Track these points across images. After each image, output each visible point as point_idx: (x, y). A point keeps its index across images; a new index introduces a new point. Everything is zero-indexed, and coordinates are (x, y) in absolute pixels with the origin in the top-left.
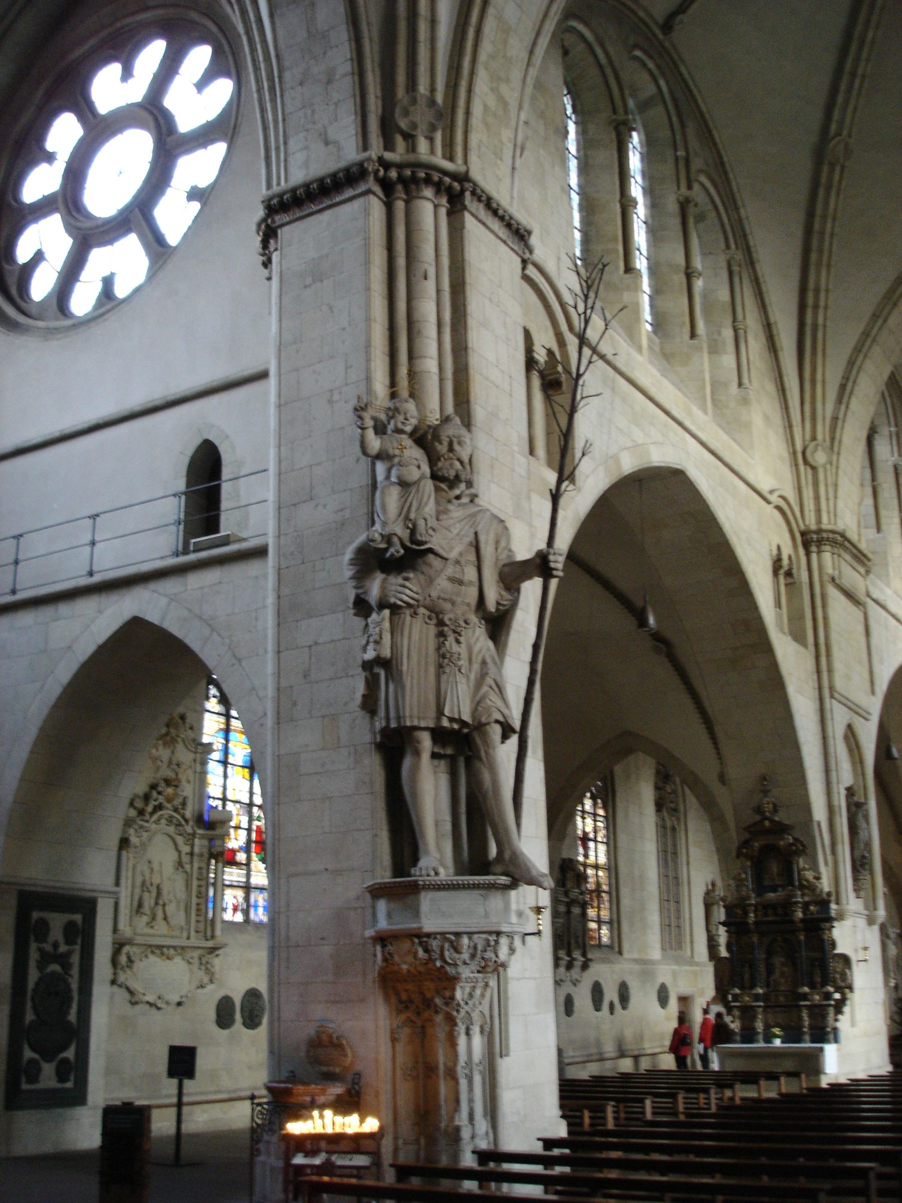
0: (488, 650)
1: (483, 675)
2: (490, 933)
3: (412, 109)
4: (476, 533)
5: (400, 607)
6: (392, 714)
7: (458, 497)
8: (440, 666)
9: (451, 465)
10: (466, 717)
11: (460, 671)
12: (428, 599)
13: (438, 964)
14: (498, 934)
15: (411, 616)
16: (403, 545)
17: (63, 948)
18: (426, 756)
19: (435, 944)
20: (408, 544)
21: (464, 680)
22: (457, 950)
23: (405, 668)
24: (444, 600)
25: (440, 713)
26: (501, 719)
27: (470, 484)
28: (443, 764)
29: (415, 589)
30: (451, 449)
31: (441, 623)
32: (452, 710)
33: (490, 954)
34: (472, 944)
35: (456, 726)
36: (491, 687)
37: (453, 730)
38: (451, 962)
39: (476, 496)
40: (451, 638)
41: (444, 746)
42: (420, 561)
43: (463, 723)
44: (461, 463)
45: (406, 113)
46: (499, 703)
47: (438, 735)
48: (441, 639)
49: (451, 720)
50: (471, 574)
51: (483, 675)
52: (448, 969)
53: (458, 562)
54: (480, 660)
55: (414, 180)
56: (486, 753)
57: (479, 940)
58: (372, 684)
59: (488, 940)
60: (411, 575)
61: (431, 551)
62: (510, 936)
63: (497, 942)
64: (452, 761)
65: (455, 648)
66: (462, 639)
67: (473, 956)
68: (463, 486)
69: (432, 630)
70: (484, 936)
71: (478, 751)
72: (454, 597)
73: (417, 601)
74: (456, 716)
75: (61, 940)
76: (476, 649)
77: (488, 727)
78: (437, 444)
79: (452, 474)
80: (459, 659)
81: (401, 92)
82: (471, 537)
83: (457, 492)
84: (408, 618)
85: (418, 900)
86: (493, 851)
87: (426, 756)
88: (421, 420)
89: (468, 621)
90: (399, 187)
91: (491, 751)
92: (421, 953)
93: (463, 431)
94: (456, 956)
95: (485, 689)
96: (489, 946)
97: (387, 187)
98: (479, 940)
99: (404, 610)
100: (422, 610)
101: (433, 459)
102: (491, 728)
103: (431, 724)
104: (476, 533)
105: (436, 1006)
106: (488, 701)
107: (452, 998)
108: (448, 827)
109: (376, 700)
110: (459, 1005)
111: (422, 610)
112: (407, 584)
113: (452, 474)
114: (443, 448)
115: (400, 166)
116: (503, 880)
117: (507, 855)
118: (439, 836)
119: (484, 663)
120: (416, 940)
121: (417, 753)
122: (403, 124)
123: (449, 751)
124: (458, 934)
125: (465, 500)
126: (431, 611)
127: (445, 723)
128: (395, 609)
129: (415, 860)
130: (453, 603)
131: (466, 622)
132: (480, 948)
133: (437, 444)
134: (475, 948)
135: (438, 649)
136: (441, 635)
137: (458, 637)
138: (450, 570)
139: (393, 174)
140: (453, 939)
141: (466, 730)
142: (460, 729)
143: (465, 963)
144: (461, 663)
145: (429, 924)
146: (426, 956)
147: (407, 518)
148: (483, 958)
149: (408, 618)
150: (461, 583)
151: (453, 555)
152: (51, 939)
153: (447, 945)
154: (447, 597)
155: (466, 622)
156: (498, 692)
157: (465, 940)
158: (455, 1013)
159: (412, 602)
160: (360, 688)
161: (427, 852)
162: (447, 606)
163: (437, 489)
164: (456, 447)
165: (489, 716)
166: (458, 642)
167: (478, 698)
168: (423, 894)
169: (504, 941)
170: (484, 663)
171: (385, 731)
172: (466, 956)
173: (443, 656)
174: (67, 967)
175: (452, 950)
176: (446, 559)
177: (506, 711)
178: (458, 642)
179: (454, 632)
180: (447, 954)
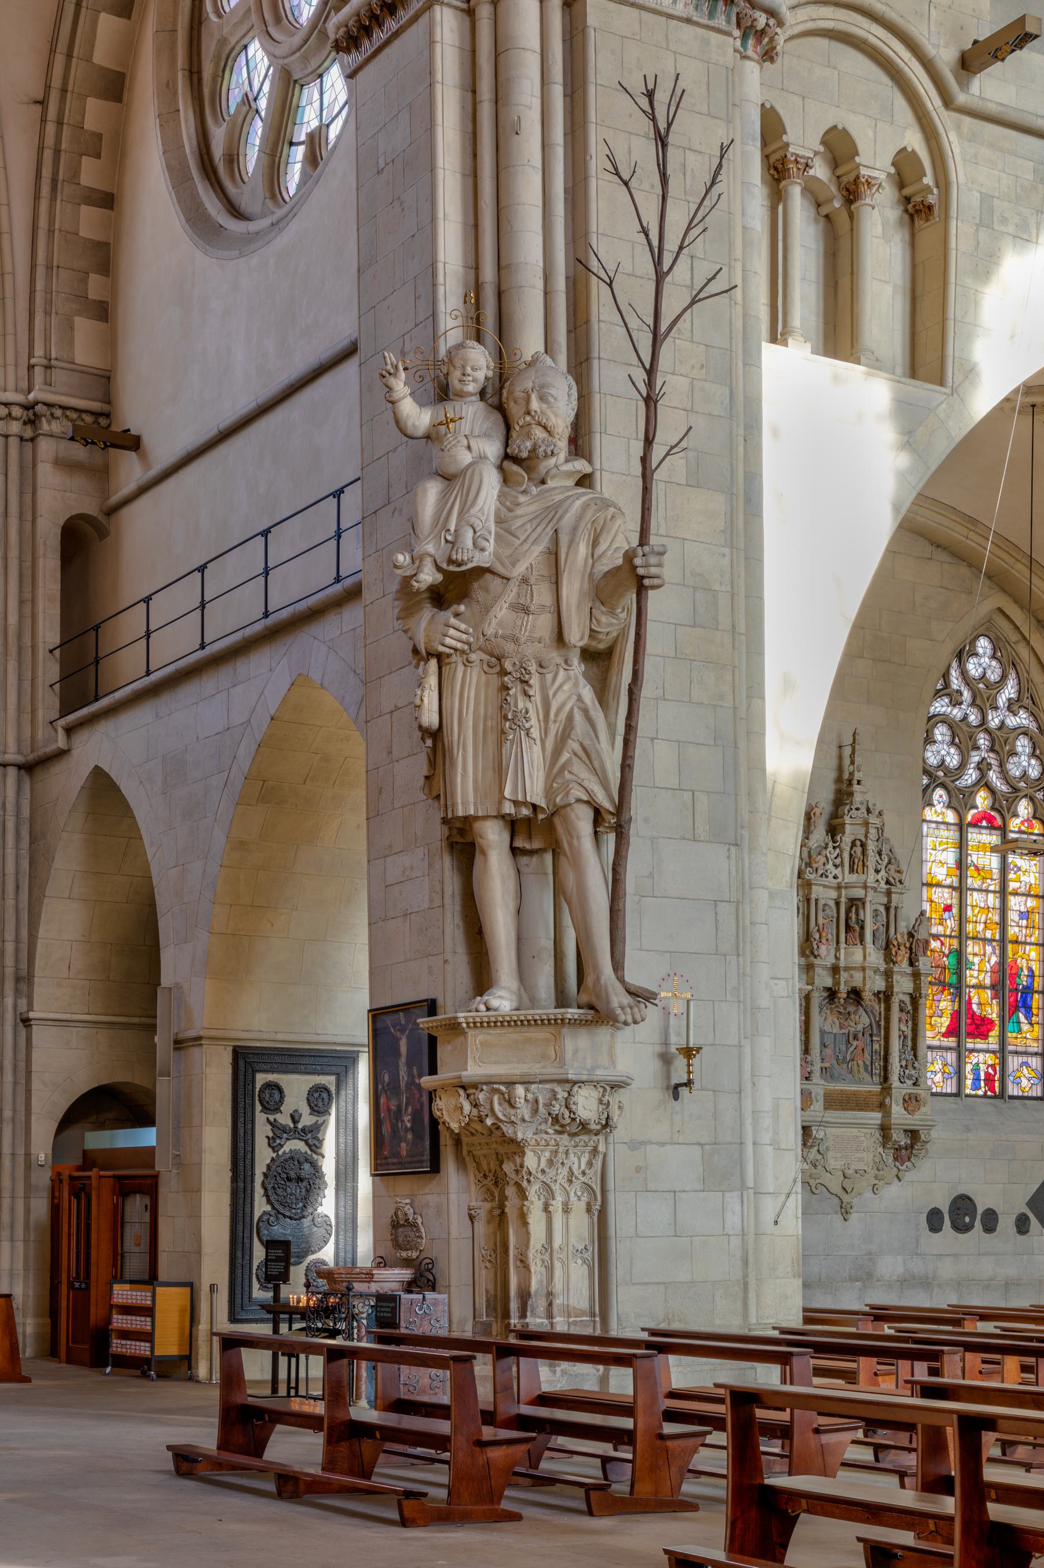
0: (580, 699)
5: (449, 656)
11: (528, 734)
12: (482, 639)
13: (489, 1122)
15: (465, 665)
16: (439, 569)
17: (307, 1120)
22: (511, 1103)
23: (456, 737)
24: (503, 637)
26: (585, 798)
29: (463, 627)
33: (556, 1109)
34: (530, 1096)
36: (575, 754)
38: (503, 1118)
43: (535, 807)
49: (516, 803)
54: (563, 716)
56: (571, 845)
59: (554, 1091)
60: (462, 608)
67: (535, 1111)
69: (495, 681)
70: (547, 1086)
73: (469, 644)
74: (520, 798)
75: (305, 1110)
77: (568, 809)
84: (461, 668)
89: (543, 664)
91: (575, 842)
92: (467, 1107)
94: (512, 1112)
95: (565, 756)
96: (556, 1099)
99: (454, 658)
102: (573, 810)
106: (566, 772)
110: (530, 1173)
120: (461, 1092)
124: (511, 1084)
126: (492, 655)
128: (439, 657)
134: (537, 1101)
137: (526, 688)
138: (511, 594)
141: (541, 816)
143: (523, 1120)
148: (550, 1114)
149: (461, 668)
152: (287, 1108)
156: (585, 758)
157: (520, 1090)
158: (525, 1184)
159: (459, 645)
162: (510, 647)
165: (567, 794)
166: (526, 694)
167: (555, 771)
172: (525, 1112)
173: (506, 718)
174: (315, 1146)
175: (506, 1105)
176: (508, 579)
178: (526, 694)
180: (496, 1107)
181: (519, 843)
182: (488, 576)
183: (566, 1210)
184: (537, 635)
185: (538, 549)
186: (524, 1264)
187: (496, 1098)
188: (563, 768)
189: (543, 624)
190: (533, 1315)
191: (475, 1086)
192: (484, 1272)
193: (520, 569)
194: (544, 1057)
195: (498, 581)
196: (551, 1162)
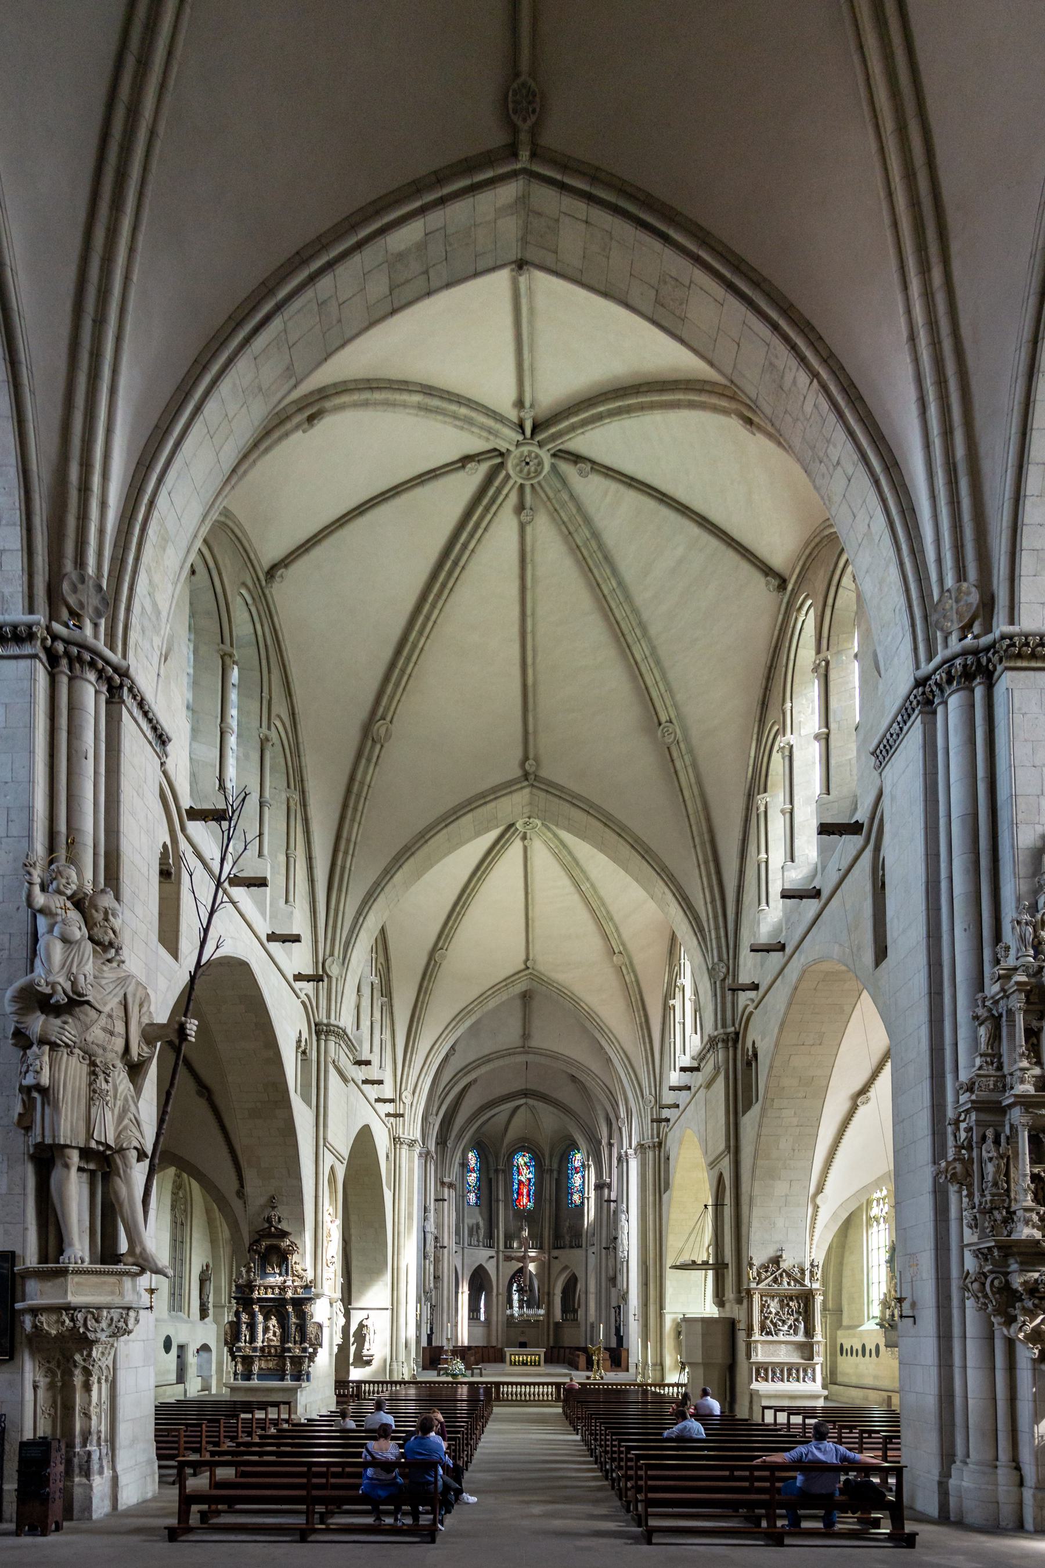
1: (124, 1111)
2: (123, 1308)
3: (80, 586)
4: (125, 995)
6: (47, 1133)
7: (109, 961)
8: (91, 1099)
9: (106, 933)
10: (111, 1143)
14: (129, 1309)
18: (74, 1170)
19: (80, 1316)
20: (71, 994)
21: (110, 1113)
25: (90, 1135)
27: (118, 950)
28: (85, 1176)
30: (106, 920)
31: (92, 1064)
32: (100, 1134)
33: (121, 1324)
35: (101, 1148)
37: (98, 1151)
39: (123, 962)
40: (102, 1077)
41: (87, 1162)
42: (77, 1009)
43: (108, 1147)
44: (114, 932)
45: (75, 590)
46: (138, 1134)
47: (86, 1153)
48: (93, 1077)
49: (98, 1143)
50: (120, 1028)
51: (124, 1111)
52: (89, 1334)
53: (110, 1016)
55: (79, 659)
57: (115, 1314)
58: (29, 1106)
61: (88, 1002)
62: (137, 1310)
63: (127, 1314)
64: (92, 1173)
65: (104, 1086)
66: (110, 1079)
67: (110, 1325)
68: (113, 951)
71: (118, 1169)
72: (105, 1044)
74: (103, 1141)
76: (120, 1089)
78: (93, 911)
79: (107, 939)
80: (107, 1095)
81: (69, 566)
82: (121, 997)
83: (109, 956)
85: (66, 1281)
86: (123, 1247)
87: (74, 1170)
88: (81, 886)
90: (64, 662)
93: (116, 904)
97: (53, 660)
98: (115, 1314)
100: (77, 1051)
101: (89, 922)
103: (82, 1145)
104: (125, 995)
105: (75, 1361)
107: (90, 1355)
108: (87, 1224)
109: (32, 1121)
111: (77, 1051)
112: (66, 1027)
113: (107, 939)
114: (99, 917)
115: (67, 642)
116: (135, 1269)
117: (138, 1250)
118: (81, 1232)
119: (126, 1100)
121: (67, 1166)
122: (72, 600)
123: (92, 1166)
125: (115, 964)
127: (93, 1145)
129: (61, 1251)
130: (104, 1049)
131: (113, 1066)
132: (115, 1319)
133: (93, 911)
134: (112, 1319)
135: (90, 1084)
136: (94, 1073)
139: (60, 647)
140: (95, 1311)
141: (108, 1152)
142: (104, 1151)
143: (103, 1330)
144: (108, 1098)
145: (73, 1299)
146: (72, 1324)
147: (70, 972)
150: (112, 1034)
151: (106, 1009)
153: (89, 1316)
154: (100, 1043)
155: (113, 1066)
160: (19, 1108)
161: (71, 1245)
162: (100, 1051)
163: (95, 951)
164: (111, 917)
166: (107, 1082)
168: (70, 1277)
169: (132, 1314)
170: (126, 1100)
171: (37, 1146)
172: (104, 1324)
177: (142, 1141)
178: (107, 1082)
179: (104, 1073)
181: (83, 1165)
182: (87, 1007)
183: (99, 1382)
184: (116, 1049)
185: (117, 1000)
186: (87, 1416)
187: (89, 1316)
188: (126, 1128)
189: (119, 1044)
190: (91, 1445)
191: (75, 1309)
192: (42, 1421)
193: (106, 1009)
194: (113, 1293)
195: (93, 1013)
196: (103, 1353)
